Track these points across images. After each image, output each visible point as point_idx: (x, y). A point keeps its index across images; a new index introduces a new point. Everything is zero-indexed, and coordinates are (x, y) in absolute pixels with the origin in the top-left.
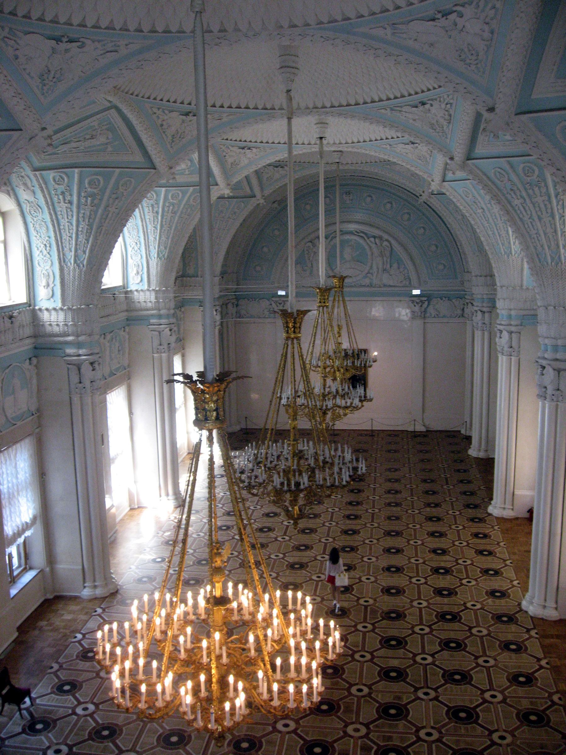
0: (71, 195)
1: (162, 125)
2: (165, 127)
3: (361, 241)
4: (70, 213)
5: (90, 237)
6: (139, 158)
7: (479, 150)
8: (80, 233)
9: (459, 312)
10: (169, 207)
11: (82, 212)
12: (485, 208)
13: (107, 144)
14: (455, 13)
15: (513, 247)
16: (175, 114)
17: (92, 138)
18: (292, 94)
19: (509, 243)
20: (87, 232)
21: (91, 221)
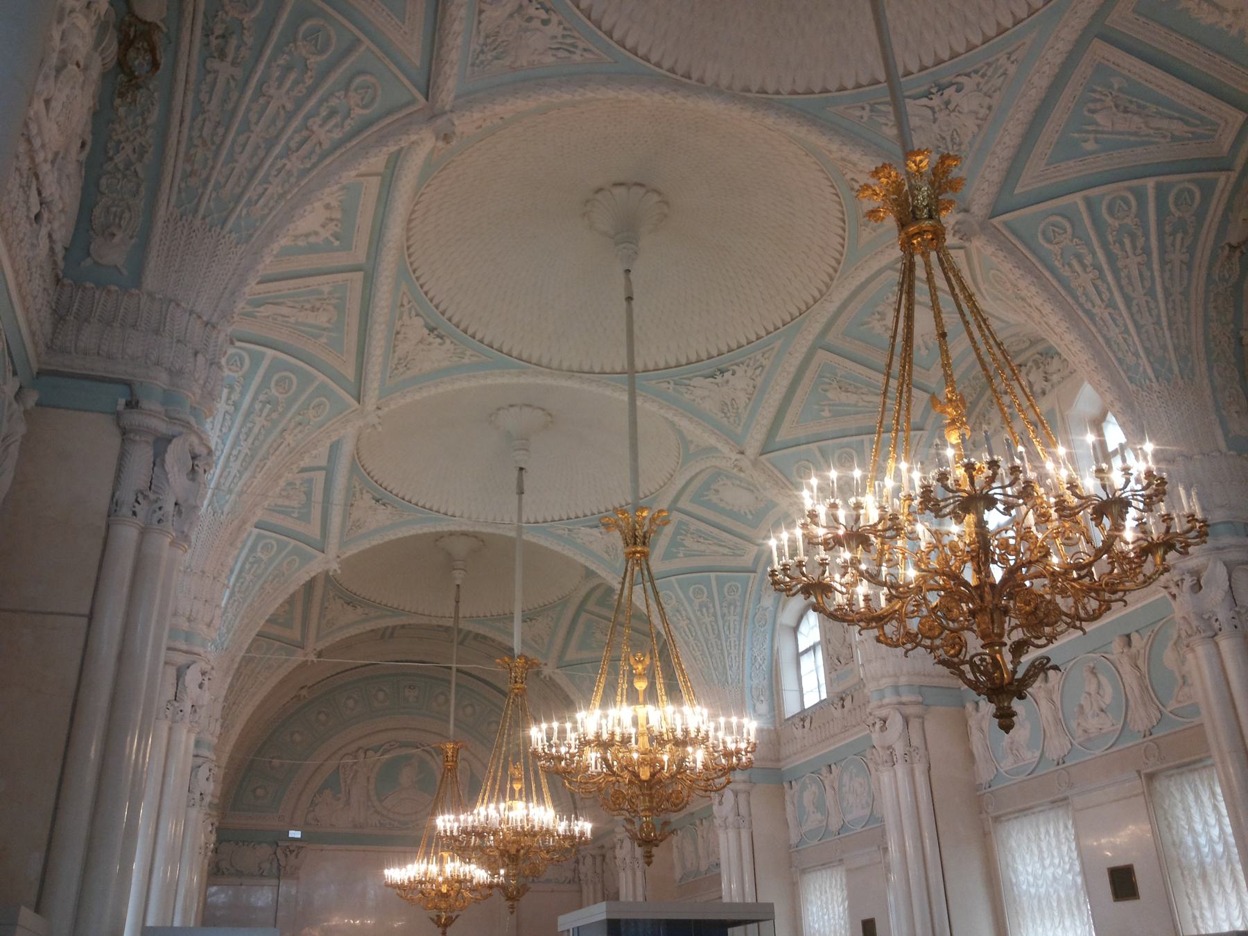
0: (242, 394)
1: (398, 333)
2: (400, 337)
3: (429, 758)
4: (228, 423)
5: (246, 469)
6: (350, 373)
7: (783, 435)
8: (232, 459)
9: (570, 875)
10: (252, 564)
11: (249, 425)
12: (693, 619)
13: (324, 329)
14: (953, 88)
15: (729, 672)
16: (419, 322)
17: (313, 309)
18: (632, 276)
19: (724, 667)
20: (244, 460)
21: (257, 443)
